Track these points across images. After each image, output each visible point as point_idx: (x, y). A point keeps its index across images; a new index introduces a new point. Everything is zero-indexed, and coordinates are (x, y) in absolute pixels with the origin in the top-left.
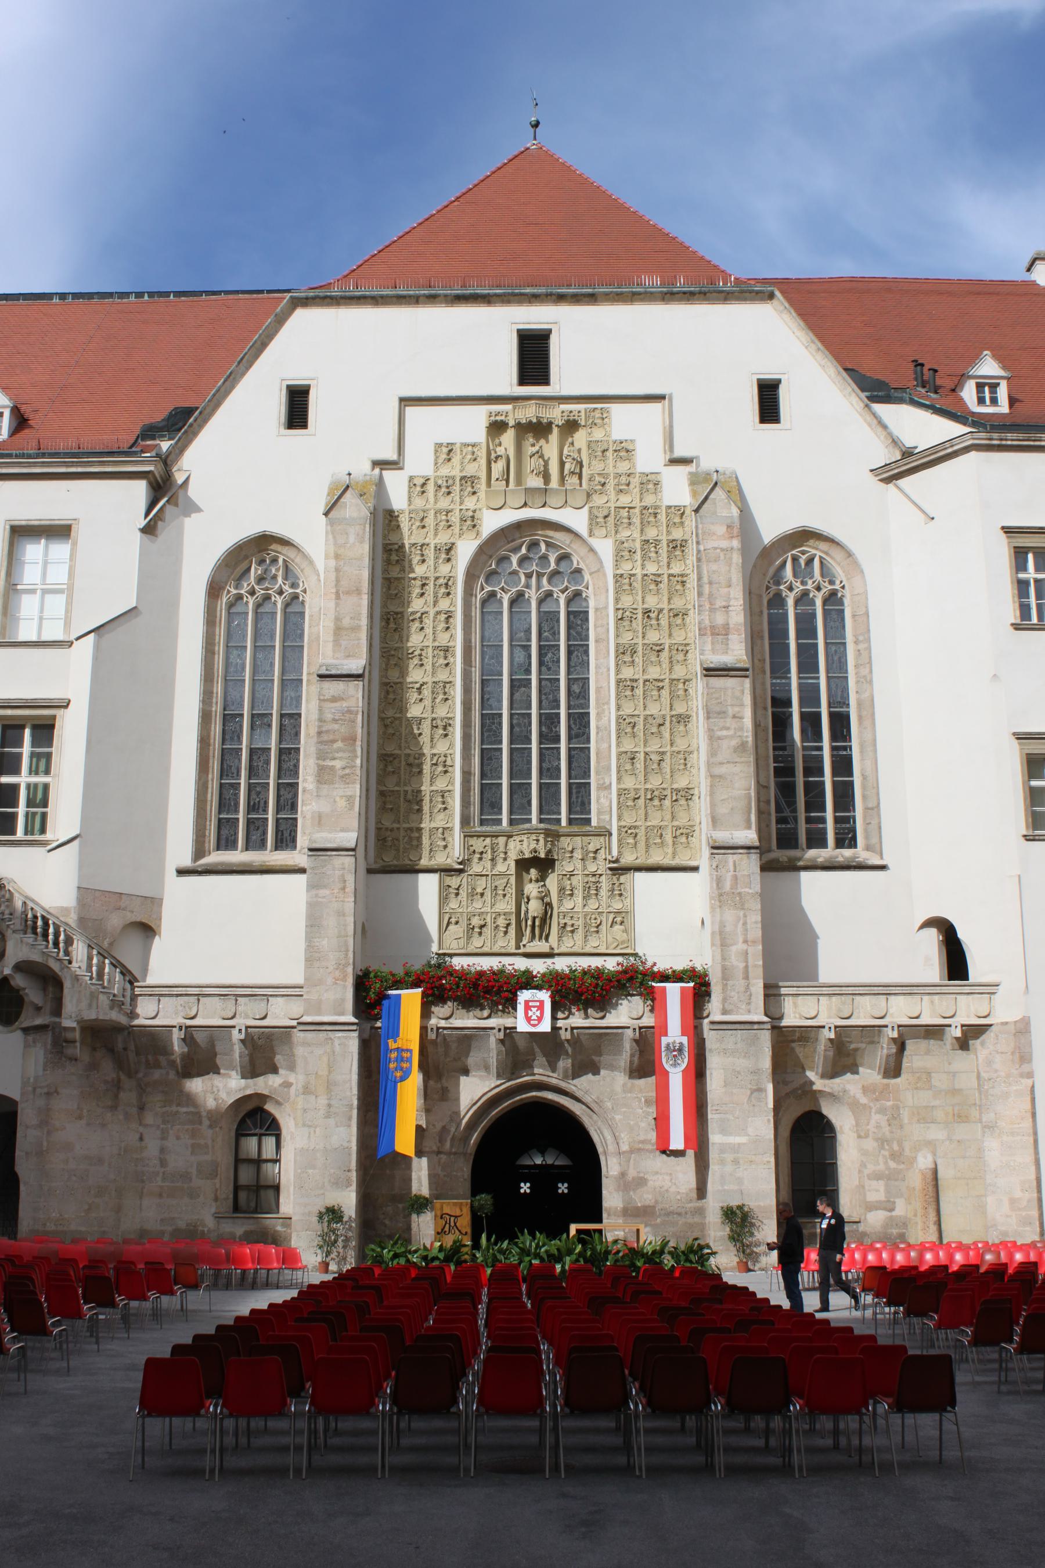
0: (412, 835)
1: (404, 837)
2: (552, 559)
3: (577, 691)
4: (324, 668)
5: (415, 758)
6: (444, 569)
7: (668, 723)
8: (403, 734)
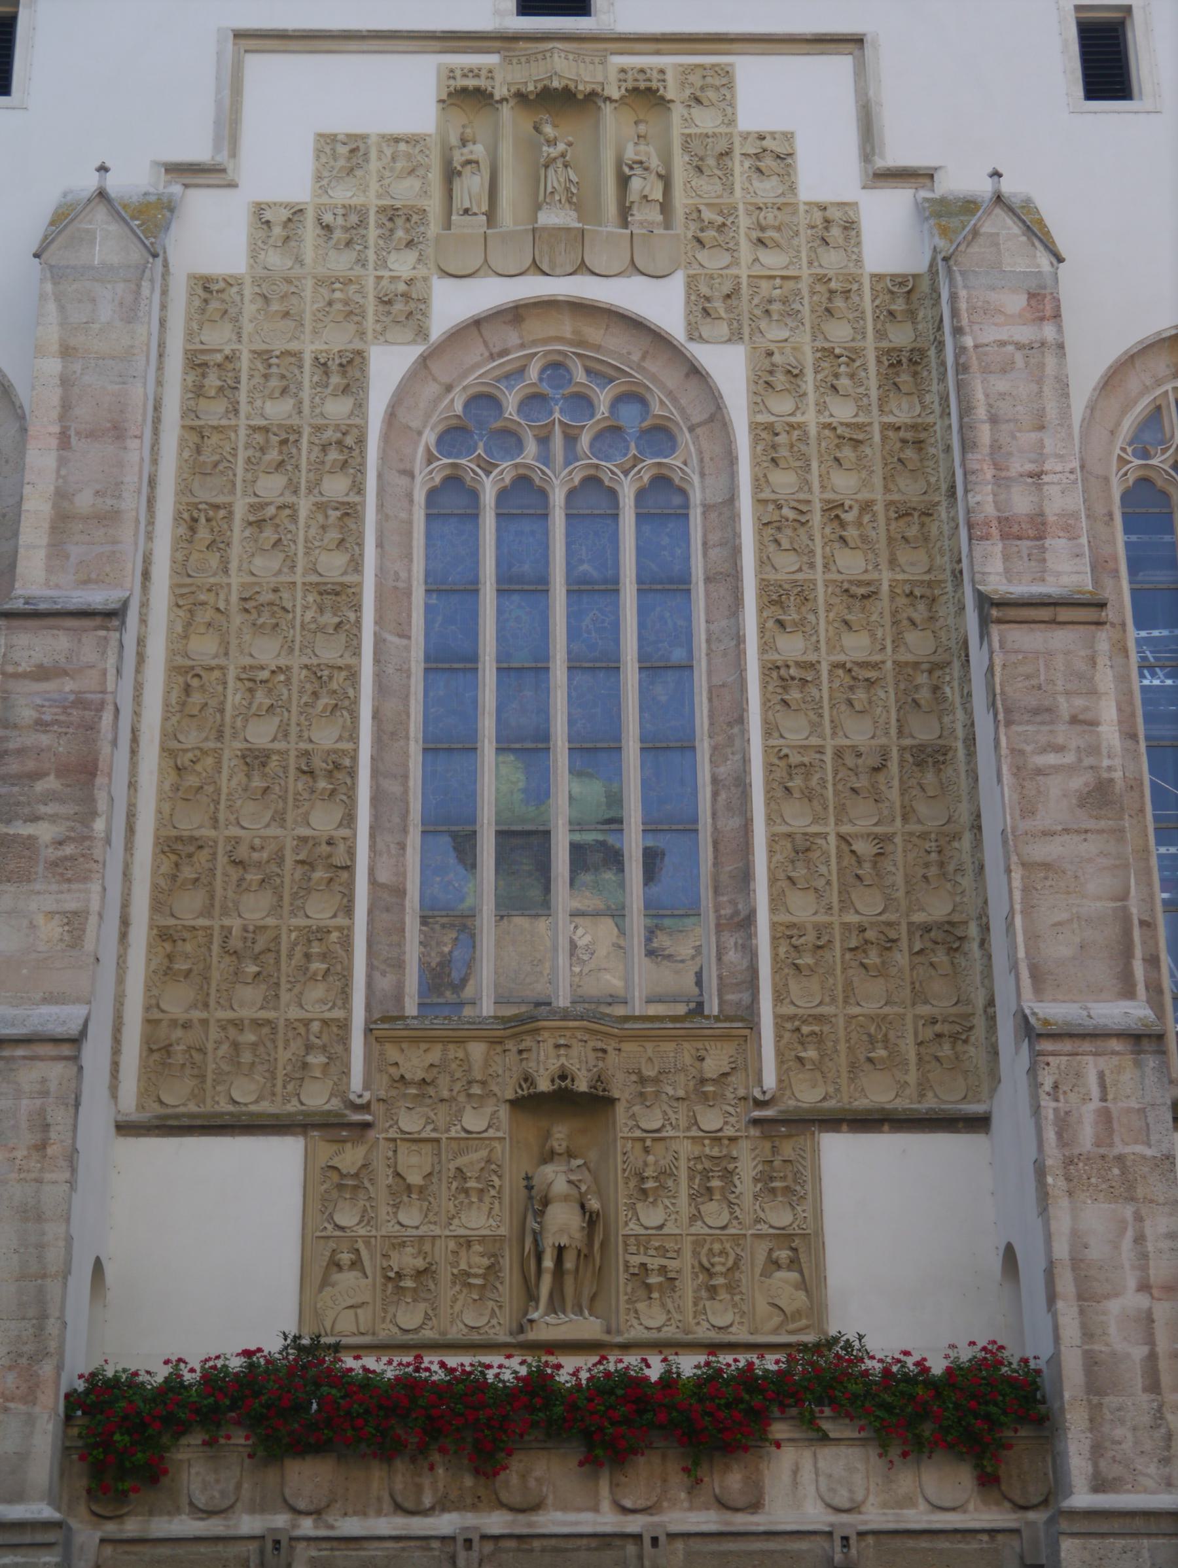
0: (241, 1039)
1: (218, 1043)
2: (603, 398)
3: (663, 699)
4: (22, 601)
5: (253, 848)
6: (338, 409)
7: (894, 766)
8: (225, 790)
